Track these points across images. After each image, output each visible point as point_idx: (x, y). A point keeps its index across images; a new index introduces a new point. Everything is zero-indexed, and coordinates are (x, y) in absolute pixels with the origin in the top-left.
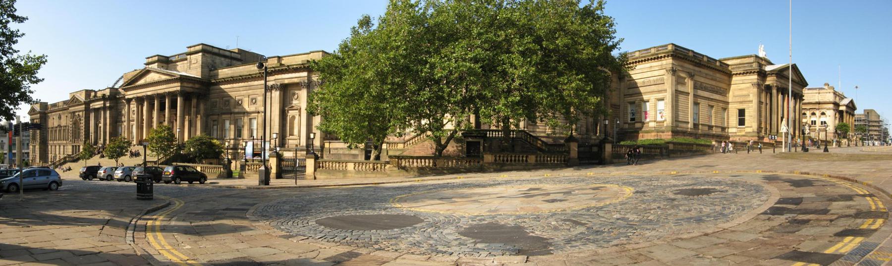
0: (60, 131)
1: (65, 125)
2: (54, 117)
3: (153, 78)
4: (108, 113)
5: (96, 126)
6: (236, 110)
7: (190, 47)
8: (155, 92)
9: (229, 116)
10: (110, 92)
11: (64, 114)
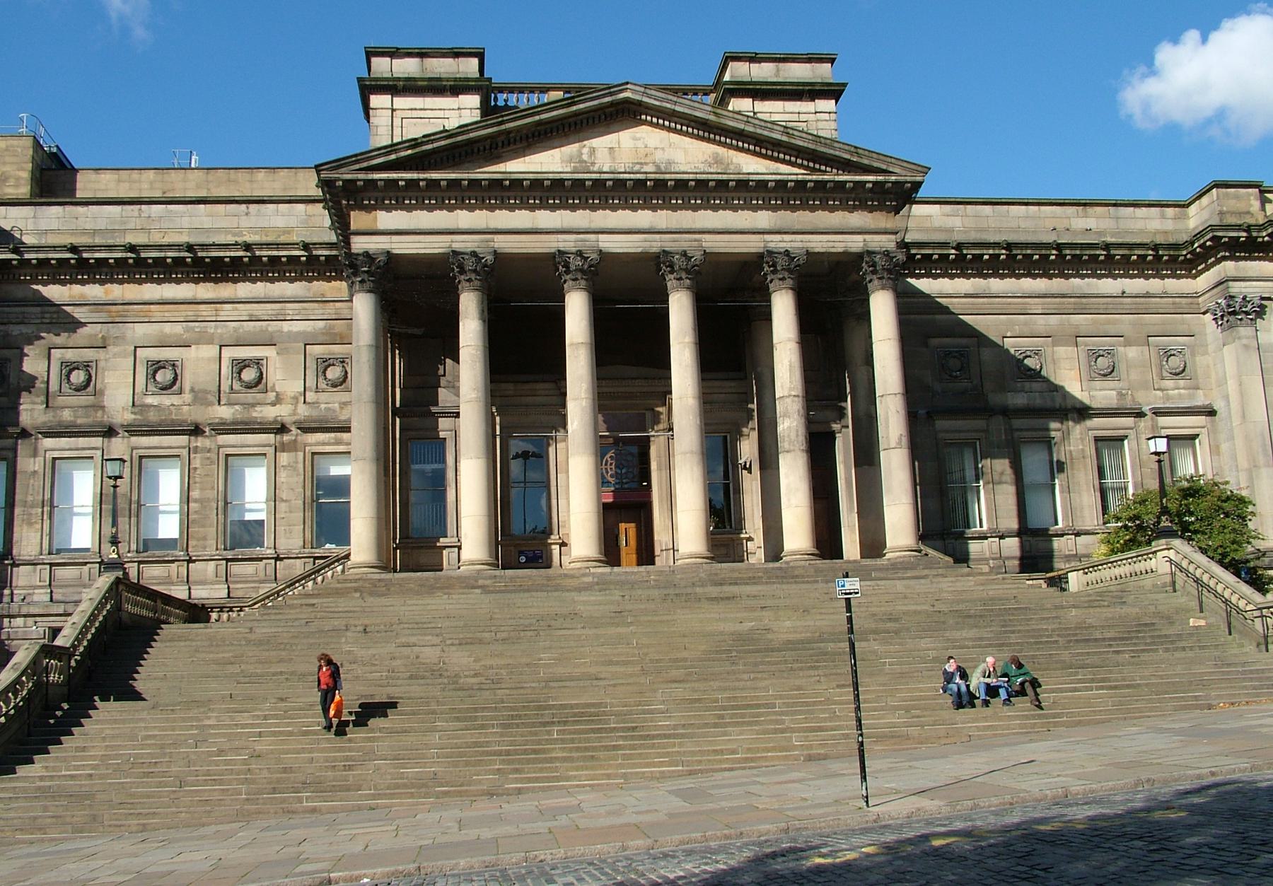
3: (659, 157)
6: (1018, 400)
8: (683, 243)
9: (979, 423)
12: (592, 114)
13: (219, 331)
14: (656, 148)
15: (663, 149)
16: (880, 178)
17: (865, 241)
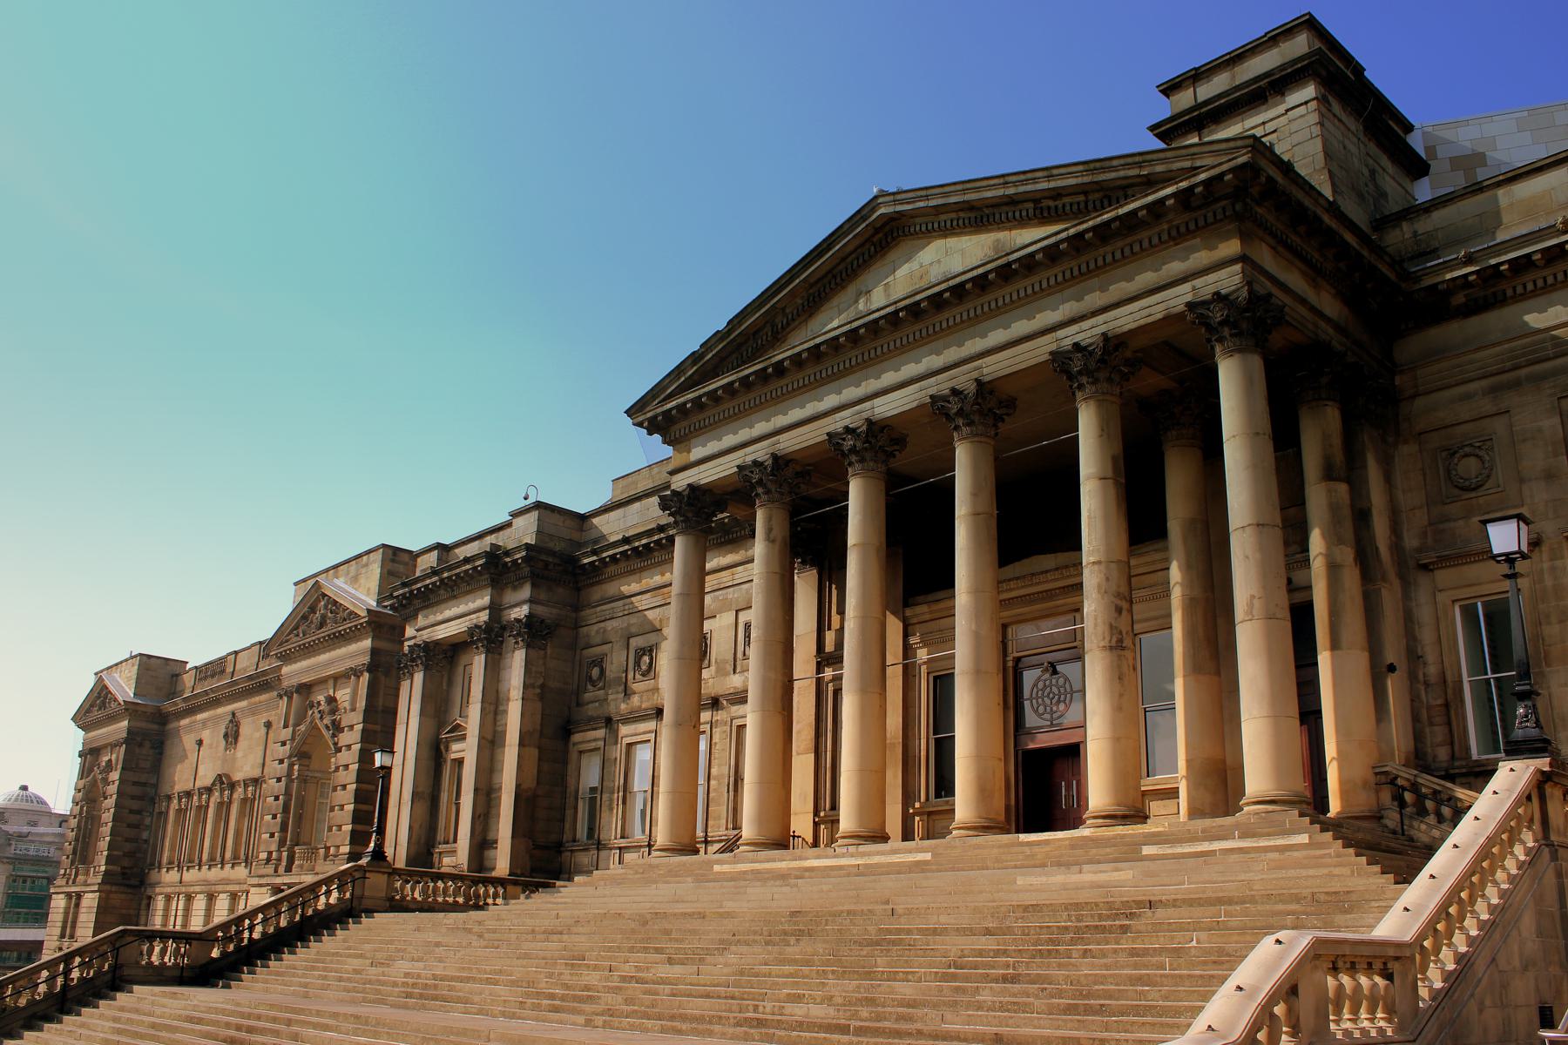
0: (224, 807)
1: (256, 773)
2: (206, 735)
4: (516, 663)
5: (435, 755)
7: (1196, 76)
8: (963, 379)
10: (539, 532)
11: (253, 711)
12: (859, 250)
13: (736, 596)
14: (931, 264)
15: (939, 261)
16: (1184, 184)
17: (1194, 289)
